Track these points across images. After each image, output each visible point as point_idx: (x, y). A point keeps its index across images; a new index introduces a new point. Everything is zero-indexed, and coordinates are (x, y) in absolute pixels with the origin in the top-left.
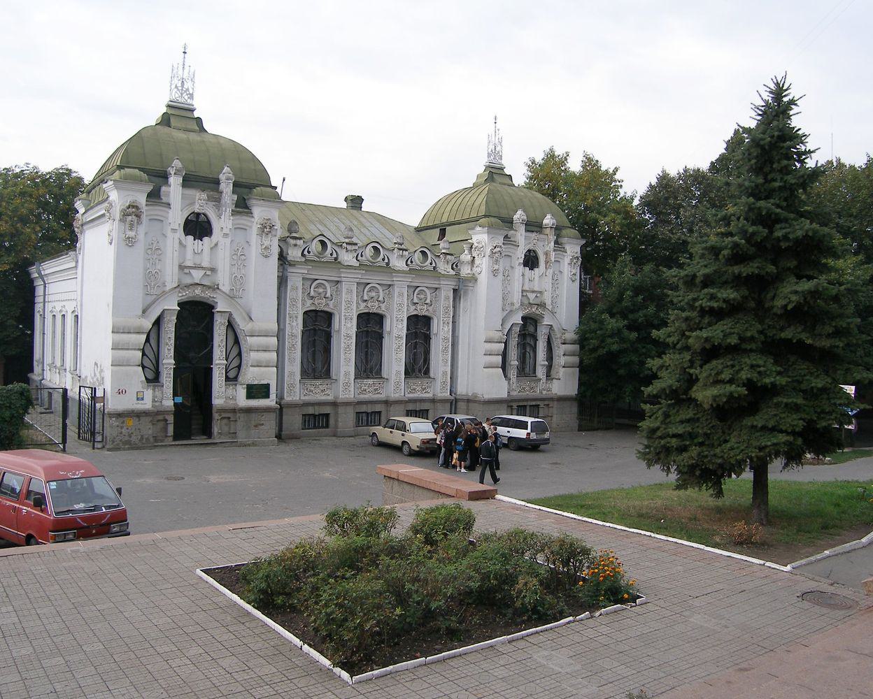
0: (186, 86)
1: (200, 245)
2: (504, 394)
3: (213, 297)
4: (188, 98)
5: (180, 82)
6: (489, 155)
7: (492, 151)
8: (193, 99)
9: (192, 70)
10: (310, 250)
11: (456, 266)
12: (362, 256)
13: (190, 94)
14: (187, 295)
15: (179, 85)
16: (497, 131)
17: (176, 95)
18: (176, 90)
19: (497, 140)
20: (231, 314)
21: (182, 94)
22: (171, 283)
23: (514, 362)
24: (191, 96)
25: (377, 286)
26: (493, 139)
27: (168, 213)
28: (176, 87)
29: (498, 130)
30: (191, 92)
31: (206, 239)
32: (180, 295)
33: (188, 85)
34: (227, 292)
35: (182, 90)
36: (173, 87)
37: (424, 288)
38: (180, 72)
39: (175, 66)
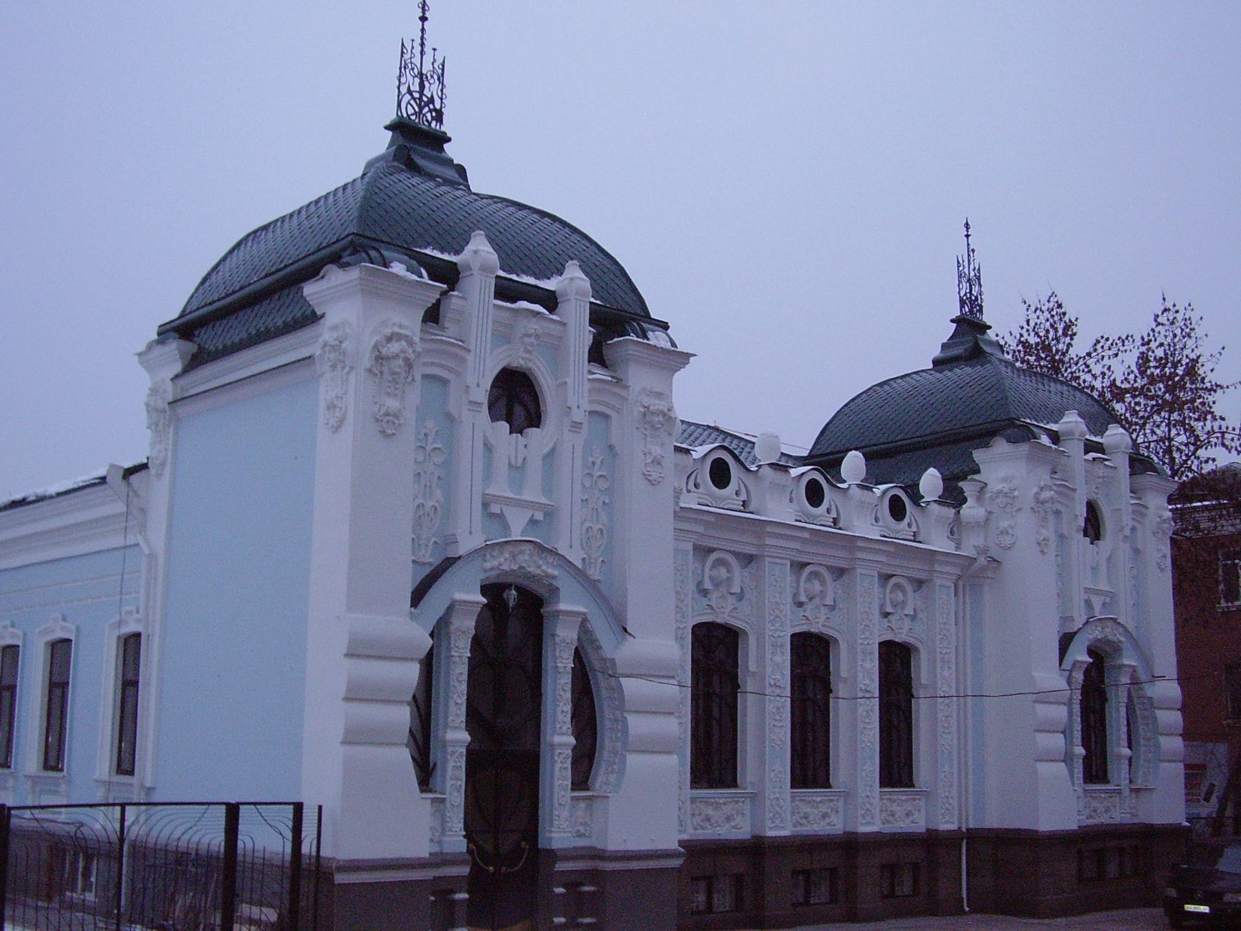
1: (521, 447)
3: (554, 577)
4: (433, 118)
5: (417, 80)
6: (962, 303)
7: (965, 295)
8: (441, 122)
9: (440, 61)
10: (699, 481)
13: (435, 110)
14: (501, 563)
15: (415, 87)
16: (971, 254)
17: (410, 110)
18: (408, 97)
19: (972, 274)
21: (421, 109)
25: (822, 570)
26: (966, 271)
28: (410, 92)
29: (973, 251)
30: (438, 107)
33: (432, 89)
36: (404, 89)
37: (901, 580)
38: (417, 61)
39: (408, 45)
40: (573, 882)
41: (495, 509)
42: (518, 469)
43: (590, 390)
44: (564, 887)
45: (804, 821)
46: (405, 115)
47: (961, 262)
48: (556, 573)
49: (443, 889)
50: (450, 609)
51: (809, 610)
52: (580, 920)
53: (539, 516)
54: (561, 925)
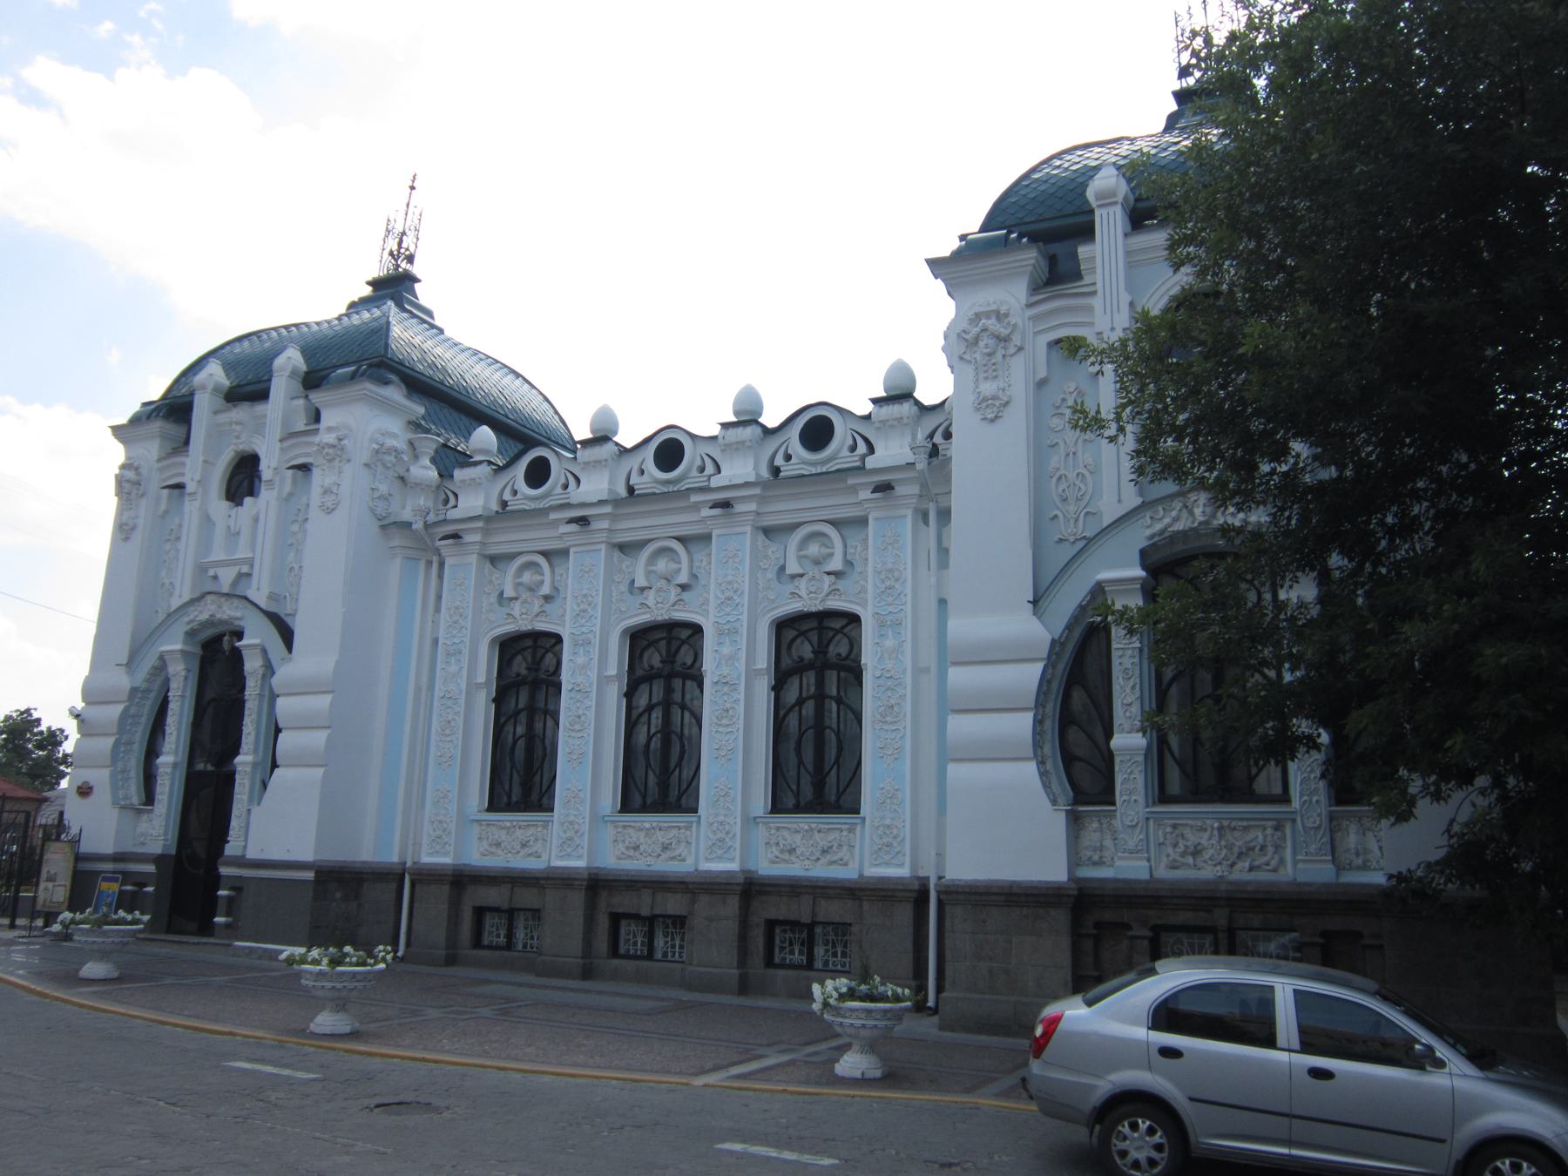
0: (404, 245)
2: (1050, 867)
3: (237, 619)
5: (397, 240)
6: (1184, 72)
11: (948, 435)
12: (642, 472)
14: (203, 613)
15: (395, 248)
20: (264, 652)
22: (183, 594)
23: (1128, 740)
24: (410, 259)
27: (183, 464)
28: (391, 253)
31: (248, 500)
32: (186, 619)
34: (263, 604)
35: (399, 252)
40: (238, 886)
41: (211, 572)
42: (233, 535)
43: (282, 449)
44: (232, 889)
45: (631, 853)
46: (385, 272)
47: (1183, 12)
48: (239, 614)
49: (140, 881)
50: (162, 658)
51: (651, 597)
52: (230, 919)
53: (245, 569)
54: (219, 924)
